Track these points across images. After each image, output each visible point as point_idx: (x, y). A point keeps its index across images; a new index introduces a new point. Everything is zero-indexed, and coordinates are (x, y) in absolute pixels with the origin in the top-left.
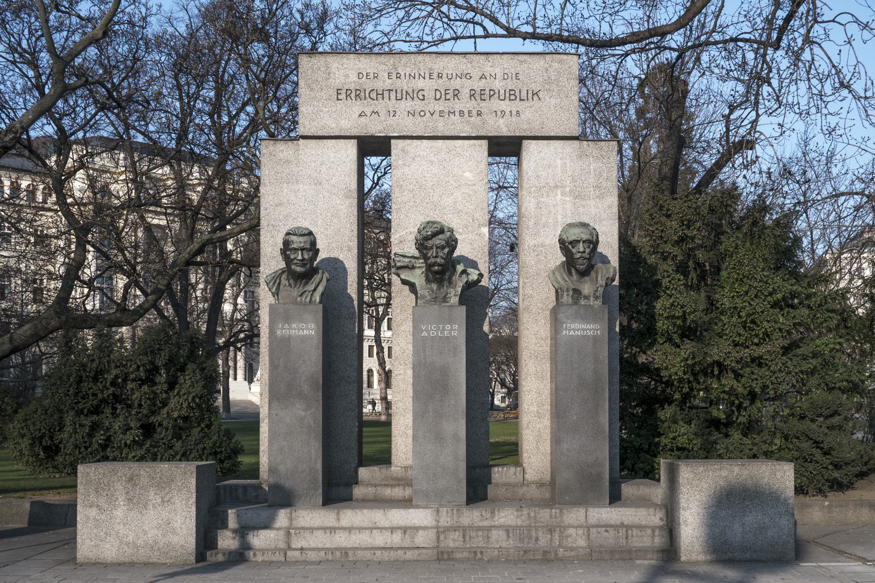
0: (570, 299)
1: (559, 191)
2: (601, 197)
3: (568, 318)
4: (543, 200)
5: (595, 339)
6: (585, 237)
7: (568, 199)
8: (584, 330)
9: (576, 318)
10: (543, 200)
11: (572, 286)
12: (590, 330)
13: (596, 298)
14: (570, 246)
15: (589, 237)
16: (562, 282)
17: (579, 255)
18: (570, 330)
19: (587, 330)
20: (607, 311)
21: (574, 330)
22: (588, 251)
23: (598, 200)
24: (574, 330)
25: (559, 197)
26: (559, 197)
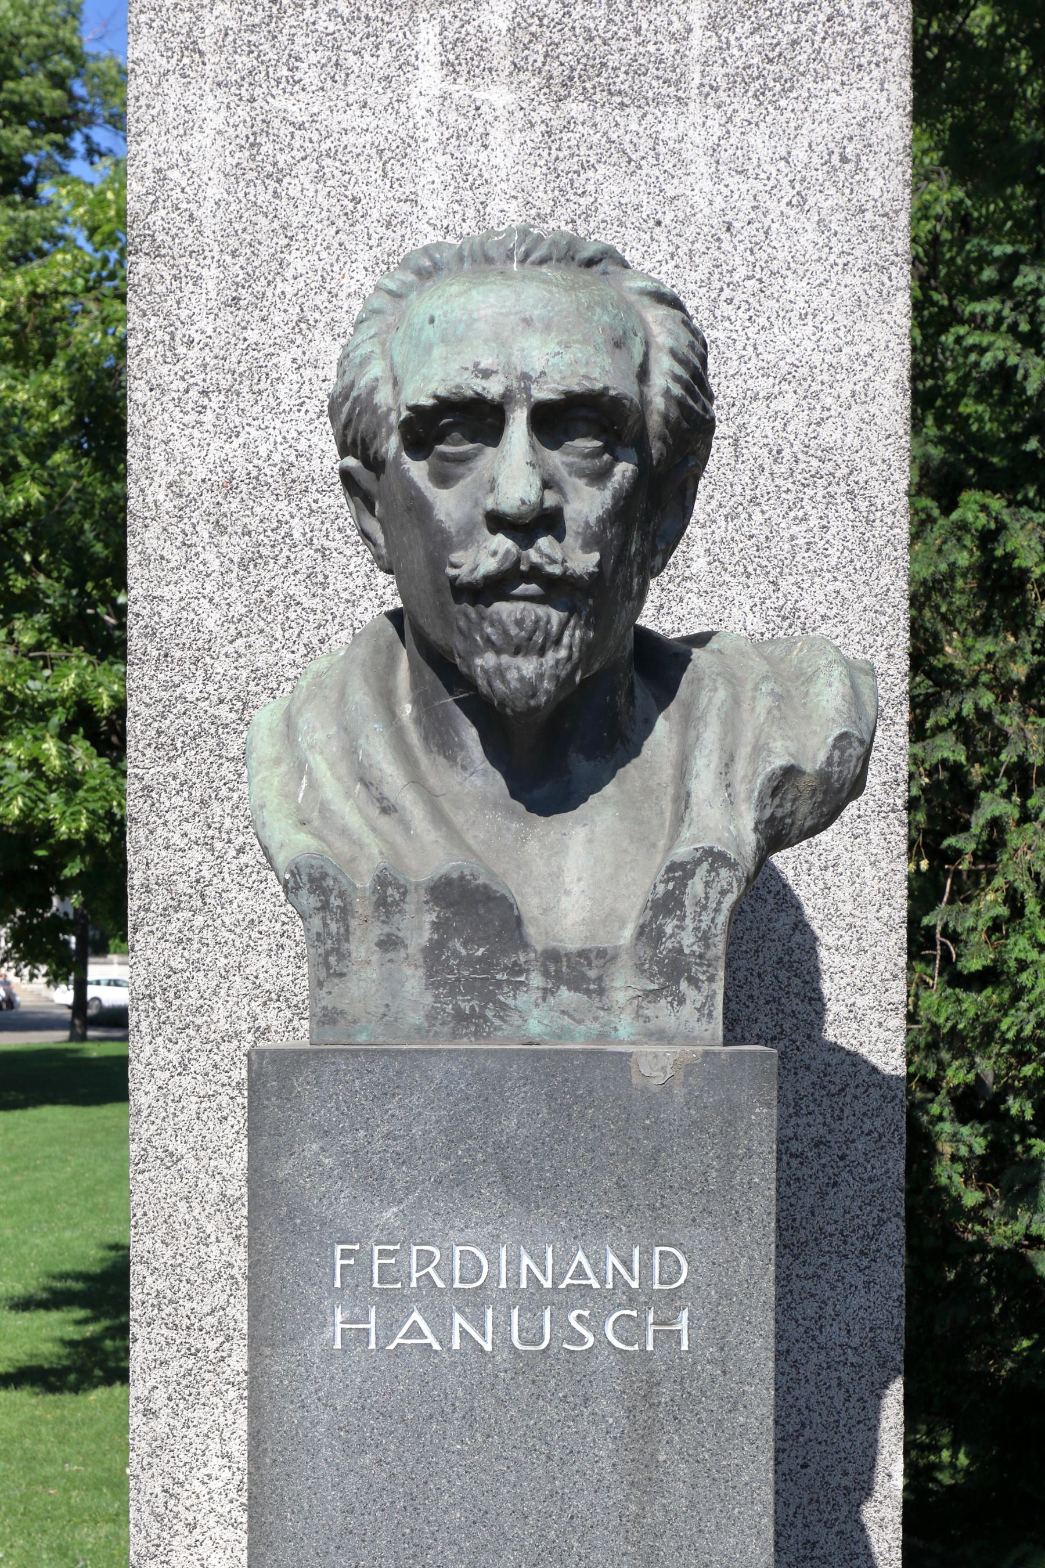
0: (413, 981)
1: (427, 38)
2: (768, 80)
3: (372, 1181)
4: (292, 105)
5: (649, 1391)
6: (558, 361)
7: (498, 96)
8: (534, 1299)
9: (460, 1180)
10: (292, 105)
11: (430, 858)
12: (599, 1301)
13: (672, 972)
14: (418, 470)
15: (597, 371)
16: (350, 812)
17: (490, 554)
18: (394, 1305)
19: (562, 1300)
20: (761, 1123)
21: (437, 1303)
22: (587, 504)
23: (744, 107)
24: (437, 1303)
25: (430, 77)
26: (430, 77)
